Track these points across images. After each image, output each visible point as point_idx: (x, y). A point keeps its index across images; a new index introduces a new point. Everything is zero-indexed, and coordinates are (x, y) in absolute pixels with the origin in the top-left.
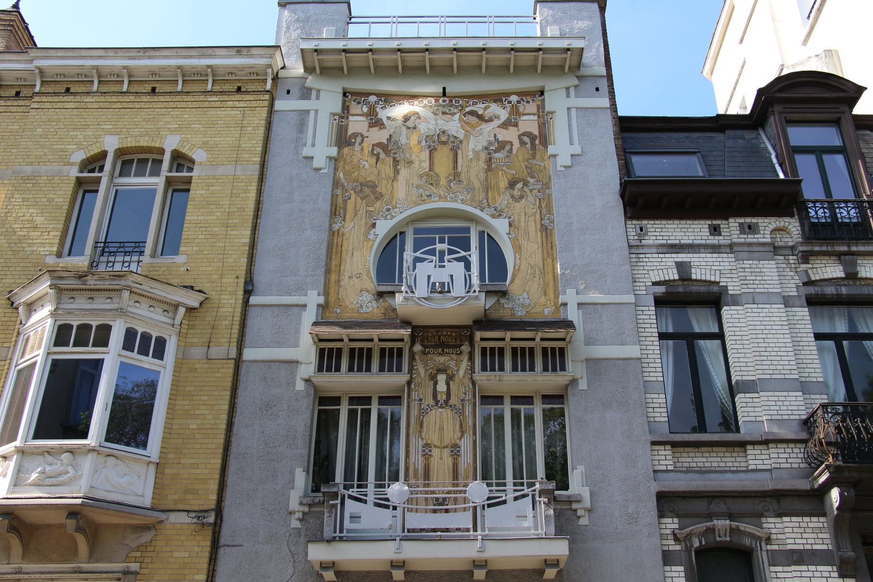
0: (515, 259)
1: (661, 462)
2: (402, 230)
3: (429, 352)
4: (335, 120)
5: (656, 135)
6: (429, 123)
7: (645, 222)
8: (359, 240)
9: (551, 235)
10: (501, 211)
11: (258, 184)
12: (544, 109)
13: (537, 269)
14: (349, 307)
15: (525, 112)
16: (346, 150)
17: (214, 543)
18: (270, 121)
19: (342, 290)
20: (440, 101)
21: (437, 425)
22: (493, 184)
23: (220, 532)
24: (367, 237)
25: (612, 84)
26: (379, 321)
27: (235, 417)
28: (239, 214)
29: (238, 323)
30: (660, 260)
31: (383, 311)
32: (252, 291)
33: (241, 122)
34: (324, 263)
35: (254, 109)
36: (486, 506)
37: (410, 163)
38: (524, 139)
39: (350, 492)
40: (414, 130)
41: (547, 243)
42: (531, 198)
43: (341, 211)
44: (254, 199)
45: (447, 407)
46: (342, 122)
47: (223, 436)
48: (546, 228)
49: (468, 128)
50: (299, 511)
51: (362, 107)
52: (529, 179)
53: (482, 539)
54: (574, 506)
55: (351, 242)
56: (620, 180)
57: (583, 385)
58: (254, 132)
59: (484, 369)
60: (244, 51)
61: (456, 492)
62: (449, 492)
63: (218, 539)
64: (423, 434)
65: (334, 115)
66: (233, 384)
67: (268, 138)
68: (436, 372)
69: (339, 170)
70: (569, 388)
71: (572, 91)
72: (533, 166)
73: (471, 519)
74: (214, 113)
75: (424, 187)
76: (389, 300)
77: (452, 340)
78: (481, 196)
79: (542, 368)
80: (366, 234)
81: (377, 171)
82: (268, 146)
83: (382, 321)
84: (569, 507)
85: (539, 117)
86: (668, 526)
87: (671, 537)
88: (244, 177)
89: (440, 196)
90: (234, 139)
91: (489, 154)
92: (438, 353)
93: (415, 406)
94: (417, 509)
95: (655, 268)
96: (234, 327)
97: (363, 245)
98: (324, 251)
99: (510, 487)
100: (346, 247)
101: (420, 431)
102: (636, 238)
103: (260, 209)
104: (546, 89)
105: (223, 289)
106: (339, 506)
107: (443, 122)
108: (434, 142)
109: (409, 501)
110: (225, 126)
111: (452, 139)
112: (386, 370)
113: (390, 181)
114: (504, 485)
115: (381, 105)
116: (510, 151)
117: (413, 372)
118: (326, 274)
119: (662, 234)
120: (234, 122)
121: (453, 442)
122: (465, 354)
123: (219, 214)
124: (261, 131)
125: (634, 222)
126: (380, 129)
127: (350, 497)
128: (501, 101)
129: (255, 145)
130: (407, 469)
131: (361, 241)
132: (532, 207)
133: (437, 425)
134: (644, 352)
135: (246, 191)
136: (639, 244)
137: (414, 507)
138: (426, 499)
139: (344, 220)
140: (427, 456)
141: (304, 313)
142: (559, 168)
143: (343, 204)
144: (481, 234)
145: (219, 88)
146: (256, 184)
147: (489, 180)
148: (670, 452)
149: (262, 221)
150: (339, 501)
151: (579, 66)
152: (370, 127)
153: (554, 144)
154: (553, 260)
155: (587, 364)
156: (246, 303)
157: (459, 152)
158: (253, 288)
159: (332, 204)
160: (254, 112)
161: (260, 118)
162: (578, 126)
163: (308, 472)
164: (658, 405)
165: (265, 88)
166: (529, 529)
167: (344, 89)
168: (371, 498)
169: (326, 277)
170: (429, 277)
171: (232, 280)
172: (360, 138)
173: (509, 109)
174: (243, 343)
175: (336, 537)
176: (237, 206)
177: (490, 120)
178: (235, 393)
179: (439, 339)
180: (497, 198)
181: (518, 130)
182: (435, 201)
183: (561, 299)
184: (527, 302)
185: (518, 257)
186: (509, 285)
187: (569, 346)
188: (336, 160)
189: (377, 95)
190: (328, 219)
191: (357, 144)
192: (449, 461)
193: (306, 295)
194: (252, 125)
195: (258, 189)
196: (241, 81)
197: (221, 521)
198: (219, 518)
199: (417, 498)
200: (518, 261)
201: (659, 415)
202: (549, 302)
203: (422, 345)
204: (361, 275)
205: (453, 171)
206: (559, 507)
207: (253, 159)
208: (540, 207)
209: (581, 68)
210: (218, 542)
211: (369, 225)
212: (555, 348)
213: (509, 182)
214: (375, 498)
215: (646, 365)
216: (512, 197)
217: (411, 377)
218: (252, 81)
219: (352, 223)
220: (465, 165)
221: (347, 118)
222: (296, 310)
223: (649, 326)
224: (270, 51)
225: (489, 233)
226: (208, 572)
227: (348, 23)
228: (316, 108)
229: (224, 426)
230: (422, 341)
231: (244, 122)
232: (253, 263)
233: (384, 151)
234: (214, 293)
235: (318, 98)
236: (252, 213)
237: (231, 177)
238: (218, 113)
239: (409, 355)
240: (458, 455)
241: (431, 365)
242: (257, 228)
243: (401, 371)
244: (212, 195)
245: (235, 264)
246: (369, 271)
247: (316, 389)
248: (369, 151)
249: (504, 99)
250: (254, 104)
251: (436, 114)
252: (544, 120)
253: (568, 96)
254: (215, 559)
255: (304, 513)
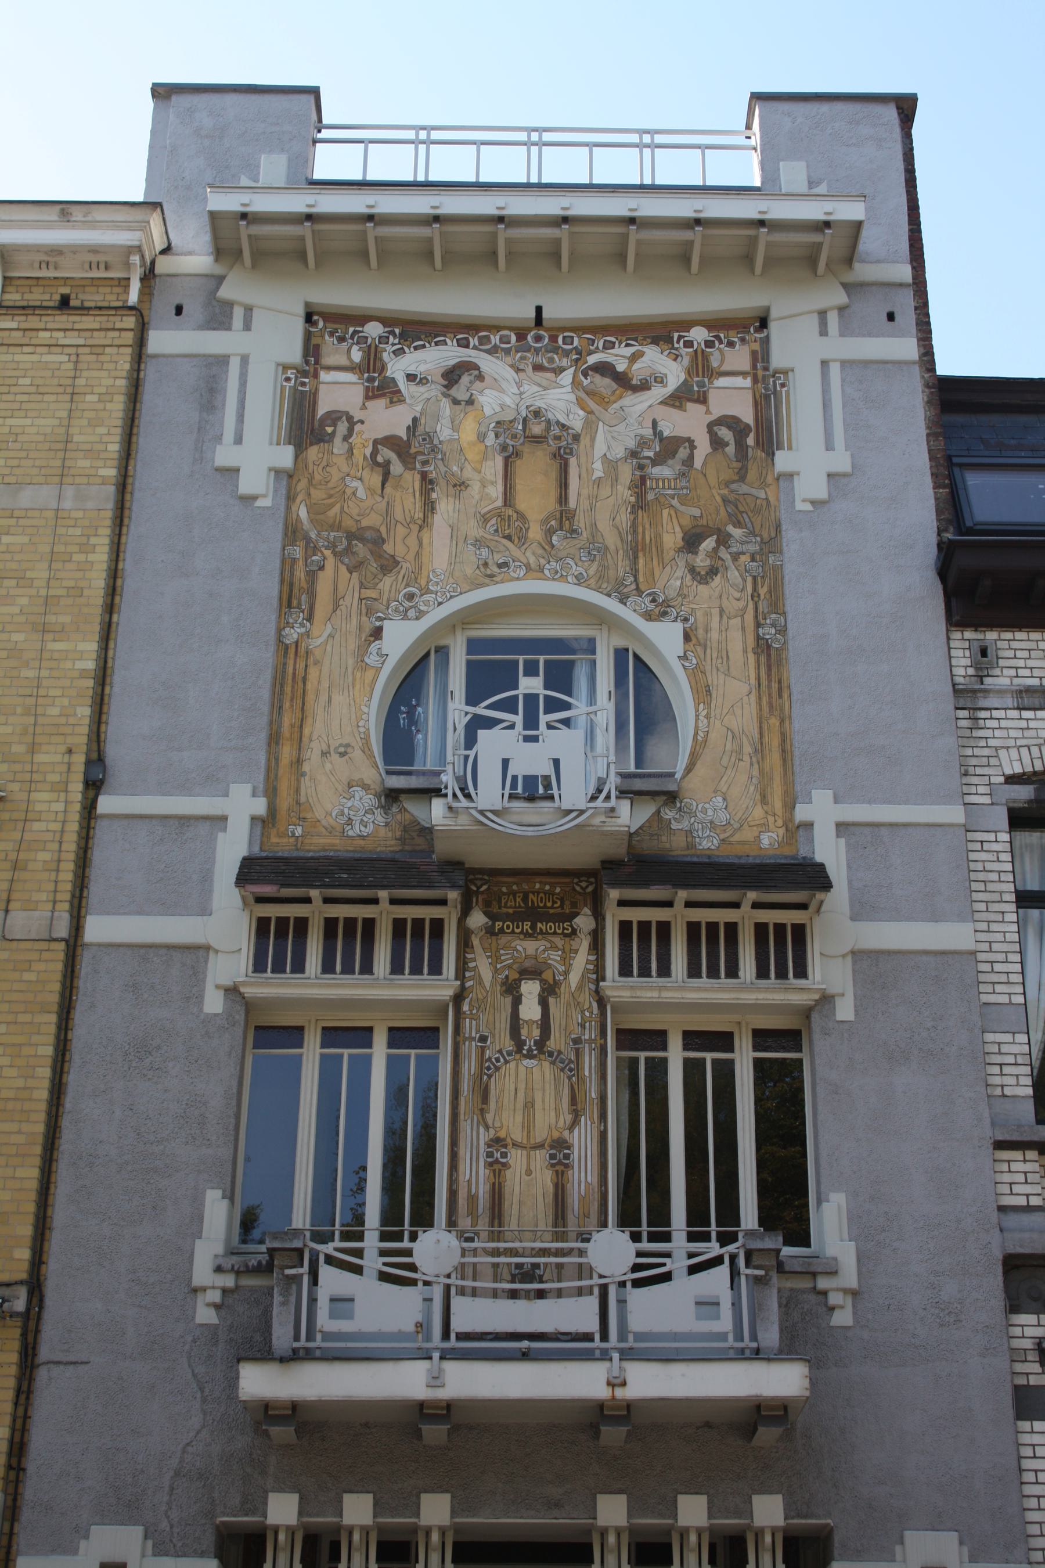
0: (697, 716)
1: (1016, 1189)
2: (443, 642)
3: (502, 931)
4: (288, 379)
5: (1023, 419)
6: (503, 391)
7: (991, 635)
8: (343, 670)
9: (779, 664)
10: (667, 603)
11: (113, 531)
12: (768, 362)
13: (745, 740)
14: (324, 822)
15: (724, 368)
16: (313, 453)
17: (26, 1355)
18: (138, 379)
19: (305, 782)
20: (529, 338)
21: (521, 1095)
22: (648, 541)
23: (37, 1331)
24: (363, 661)
25: (926, 304)
26: (390, 855)
27: (68, 1073)
28: (70, 601)
29: (72, 856)
30: (1024, 724)
31: (398, 834)
32: (102, 782)
33: (69, 382)
34: (265, 720)
35: (99, 350)
36: (629, 1284)
37: (461, 485)
38: (720, 433)
39: (329, 1248)
40: (470, 408)
41: (770, 680)
42: (734, 574)
43: (304, 597)
44: (105, 566)
45: (542, 1057)
46: (303, 384)
47: (42, 1117)
48: (769, 647)
49: (592, 405)
50: (214, 1288)
51: (349, 350)
52: (730, 529)
53: (620, 1359)
54: (822, 1283)
55: (325, 670)
56: (939, 534)
57: (845, 1010)
58: (100, 406)
59: (625, 970)
60: (77, 214)
61: (559, 1253)
62: (544, 1252)
63: (34, 1348)
64: (489, 1117)
65: (285, 367)
66: (62, 995)
67: (133, 420)
68: (517, 976)
69: (298, 500)
70: (815, 1016)
71: (833, 318)
72: (741, 499)
73: (597, 1311)
74: (9, 357)
75: (492, 544)
76: (414, 808)
77: (554, 902)
78: (623, 566)
79: (754, 970)
80: (362, 651)
81: (384, 504)
82: (134, 439)
83: (397, 856)
84: (810, 1285)
85: (755, 381)
86: (1029, 1332)
87: (1033, 1356)
88: (80, 514)
89: (528, 567)
90: (56, 422)
91: (641, 467)
92: (522, 932)
93: (470, 1051)
94: (474, 1289)
95: (1011, 743)
96: (63, 866)
97: (354, 680)
98: (266, 694)
99: (679, 1242)
100: (316, 683)
101: (482, 1110)
102: (971, 671)
103: (118, 589)
104: (774, 314)
105: (36, 777)
106: (306, 1279)
107: (536, 388)
108: (514, 436)
109: (461, 1269)
110: (33, 389)
111: (556, 431)
112: (407, 970)
113: (417, 528)
114: (666, 1237)
115: (393, 345)
116: (689, 461)
117: (467, 974)
118: (269, 745)
119: (1030, 663)
120: (55, 381)
121: (556, 1135)
122: (582, 936)
123: (24, 601)
124: (118, 406)
125: (969, 634)
126: (391, 402)
127: (330, 1260)
128: (669, 340)
129: (105, 439)
130: (453, 1195)
131: (350, 670)
132: (737, 595)
133: (521, 1095)
134: (982, 936)
135: (86, 548)
136: (978, 687)
137: (469, 1283)
138: (495, 1266)
139: (310, 618)
140: (497, 1167)
141: (221, 835)
142: (800, 506)
143: (307, 582)
144: (621, 654)
145: (18, 297)
146: (108, 531)
147: (640, 530)
148: (1036, 1167)
149: (122, 619)
150: (306, 1268)
151: (850, 260)
152: (367, 398)
153: (790, 448)
154: (782, 721)
155: (854, 963)
156: (89, 809)
157: (573, 462)
158: (104, 776)
159: (282, 581)
160: (102, 358)
161: (113, 373)
162: (844, 406)
163: (232, 1200)
164: (1011, 1059)
165: (127, 301)
166: (722, 1337)
167: (307, 305)
168: (372, 1262)
169: (269, 753)
170: (506, 763)
171: (58, 758)
172: (346, 424)
173: (686, 361)
174: (84, 904)
175: (299, 1349)
176: (66, 583)
177: (644, 386)
178: (68, 1019)
179: (525, 899)
180: (657, 573)
181: (708, 412)
182: (518, 579)
183: (802, 813)
184: (723, 817)
185: (704, 713)
186: (683, 777)
187: (817, 921)
188: (290, 476)
189: (385, 321)
190: (274, 617)
191: (338, 440)
192: (546, 1179)
193: (227, 795)
194: (97, 390)
195: (112, 542)
196: (69, 282)
197: (41, 1307)
198: (35, 1300)
199: (475, 1265)
200: (703, 722)
201: (1012, 1081)
202: (771, 819)
203: (486, 914)
204: (349, 750)
205: (558, 506)
206: (789, 1285)
207: (103, 472)
208: (755, 595)
209: (856, 265)
210: (35, 1355)
211: (368, 628)
212: (784, 926)
213: (685, 534)
214: (385, 1264)
215: (986, 967)
216: (692, 570)
217: (462, 986)
218: (95, 283)
219: (329, 625)
220: (585, 492)
221: (316, 376)
222: (203, 828)
223: (994, 877)
224: (138, 215)
225: (638, 652)
226: (14, 1421)
227: (315, 142)
228: (245, 351)
229: (44, 1094)
230: (487, 904)
231: (78, 382)
232: (104, 718)
233: (400, 455)
234: (15, 787)
235: (247, 327)
236: (100, 601)
237: (50, 514)
238: (17, 358)
239: (458, 936)
240: (567, 1166)
241: (507, 959)
242: (112, 636)
243: (440, 974)
244: (8, 556)
245: (63, 720)
246: (366, 739)
247: (249, 1006)
248: (365, 457)
249: (676, 335)
250: (99, 338)
251: (518, 370)
252: (766, 389)
253: (823, 332)
254: (29, 1392)
255: (225, 1291)
